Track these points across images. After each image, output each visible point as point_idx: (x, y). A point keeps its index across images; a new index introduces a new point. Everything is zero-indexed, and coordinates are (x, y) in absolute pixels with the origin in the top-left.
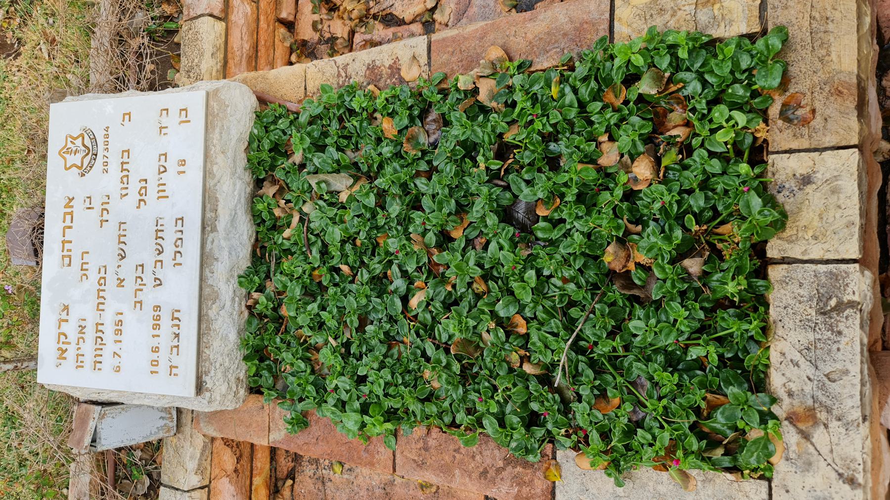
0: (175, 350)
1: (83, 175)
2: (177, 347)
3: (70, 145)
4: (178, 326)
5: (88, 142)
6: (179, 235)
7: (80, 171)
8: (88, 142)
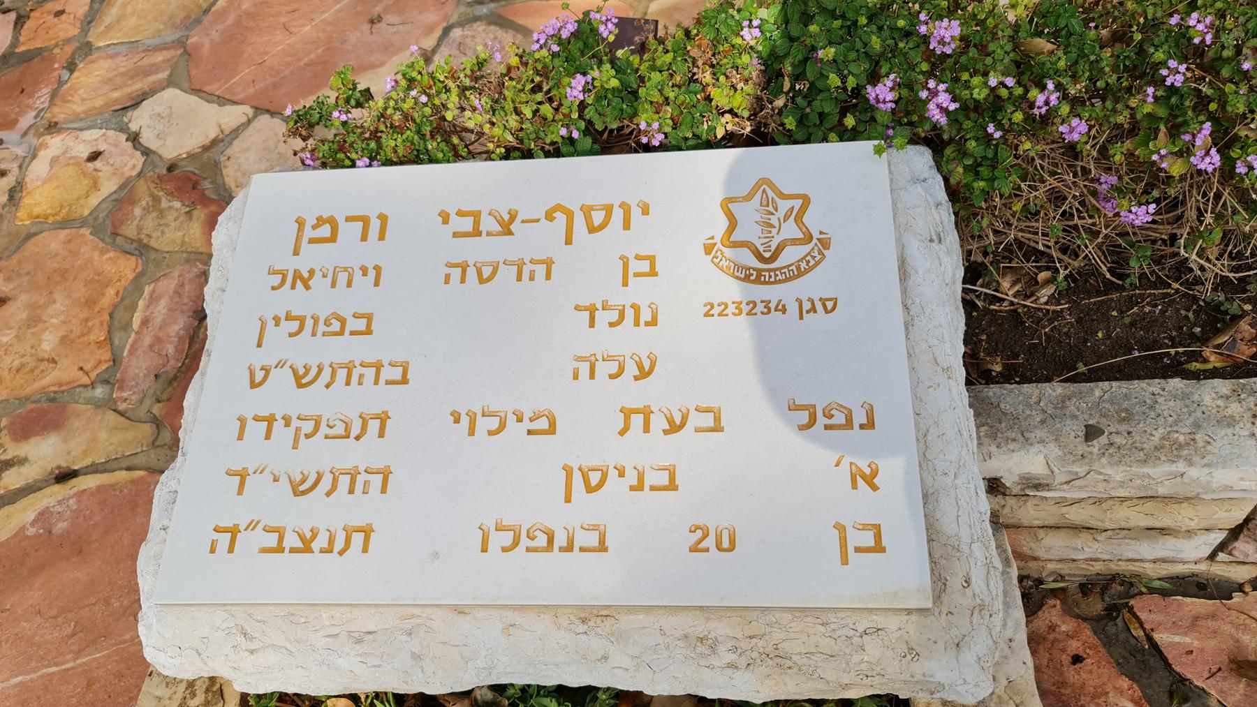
0: (272, 540)
1: (708, 249)
2: (279, 549)
3: (784, 206)
4: (329, 550)
5: (791, 255)
6: (560, 540)
7: (718, 240)
8: (791, 255)
